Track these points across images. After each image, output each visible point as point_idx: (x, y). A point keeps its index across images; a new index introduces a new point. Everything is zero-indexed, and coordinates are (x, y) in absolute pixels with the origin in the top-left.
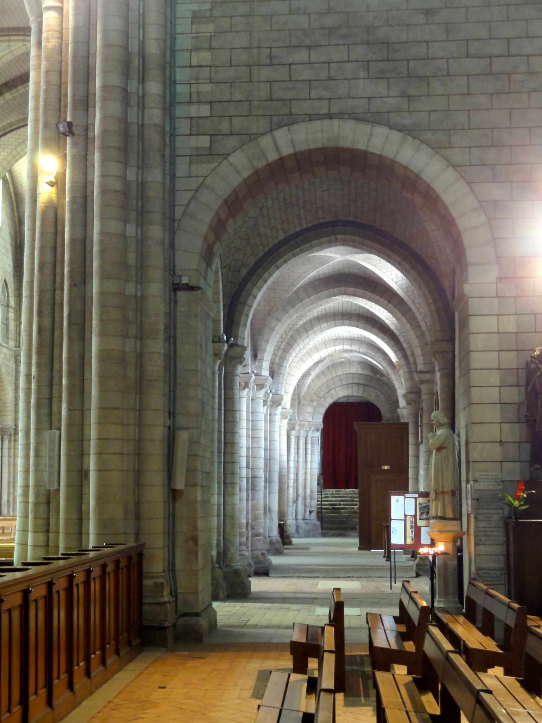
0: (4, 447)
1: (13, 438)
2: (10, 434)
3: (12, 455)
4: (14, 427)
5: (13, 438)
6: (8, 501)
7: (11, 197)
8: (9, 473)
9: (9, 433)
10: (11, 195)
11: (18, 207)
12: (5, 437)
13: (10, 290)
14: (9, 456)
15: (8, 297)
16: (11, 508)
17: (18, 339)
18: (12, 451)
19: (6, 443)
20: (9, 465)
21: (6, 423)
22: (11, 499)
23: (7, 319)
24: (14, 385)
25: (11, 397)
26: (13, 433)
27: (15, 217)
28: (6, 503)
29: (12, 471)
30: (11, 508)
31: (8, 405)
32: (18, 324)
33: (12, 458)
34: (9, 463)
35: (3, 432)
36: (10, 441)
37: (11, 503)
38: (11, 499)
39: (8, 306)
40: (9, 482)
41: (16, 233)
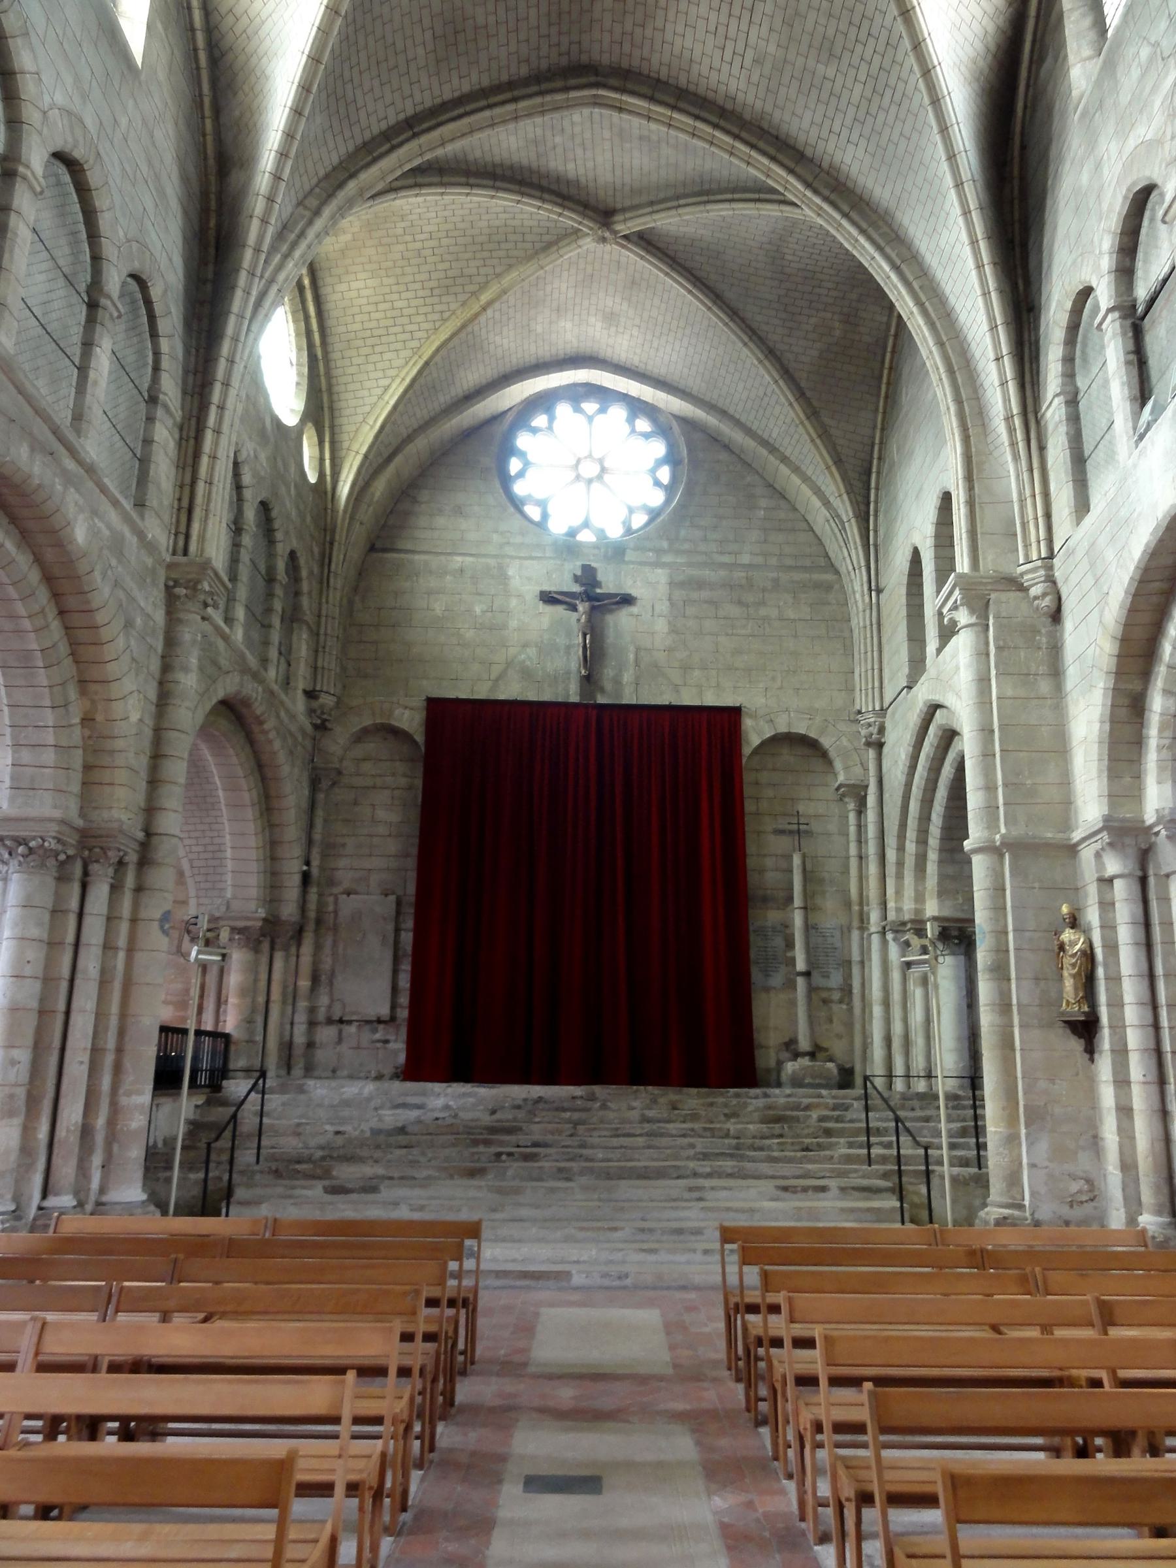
0: (88, 908)
1: (130, 881)
2: (121, 863)
3: (122, 942)
4: (140, 835)
5: (130, 881)
6: (86, 1131)
7: (195, 50)
8: (100, 1016)
9: (113, 856)
10: (194, 39)
11: (217, 111)
12: (94, 868)
13: (164, 345)
14: (108, 946)
15: (156, 368)
16: (97, 1160)
17: (183, 529)
18: (124, 928)
19: (100, 893)
20: (104, 982)
21: (106, 814)
22: (100, 1122)
23: (148, 442)
24: (155, 684)
25: (135, 717)
26: (132, 858)
27: (204, 135)
28: (74, 1139)
29: (115, 1009)
30: (97, 1160)
31: (120, 744)
32: (188, 480)
33: (121, 955)
34: (103, 971)
35: (90, 850)
36: (116, 888)
37: (100, 1138)
38: (100, 1122)
39: (153, 399)
40: (96, 1051)
41: (204, 194)
